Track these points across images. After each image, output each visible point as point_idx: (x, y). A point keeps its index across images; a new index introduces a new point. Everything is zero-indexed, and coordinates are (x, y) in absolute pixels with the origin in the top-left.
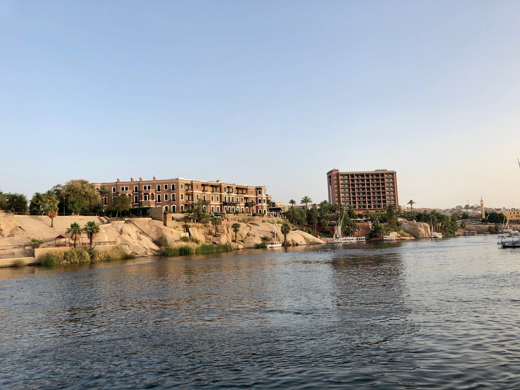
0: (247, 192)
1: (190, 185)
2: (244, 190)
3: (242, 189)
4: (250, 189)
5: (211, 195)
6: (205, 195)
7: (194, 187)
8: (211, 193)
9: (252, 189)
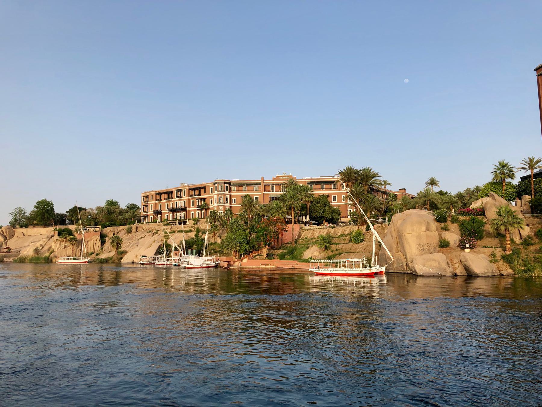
0: (205, 192)
1: (148, 196)
2: (201, 190)
3: (199, 189)
4: (209, 187)
5: (166, 204)
6: (161, 204)
7: (150, 197)
8: (165, 201)
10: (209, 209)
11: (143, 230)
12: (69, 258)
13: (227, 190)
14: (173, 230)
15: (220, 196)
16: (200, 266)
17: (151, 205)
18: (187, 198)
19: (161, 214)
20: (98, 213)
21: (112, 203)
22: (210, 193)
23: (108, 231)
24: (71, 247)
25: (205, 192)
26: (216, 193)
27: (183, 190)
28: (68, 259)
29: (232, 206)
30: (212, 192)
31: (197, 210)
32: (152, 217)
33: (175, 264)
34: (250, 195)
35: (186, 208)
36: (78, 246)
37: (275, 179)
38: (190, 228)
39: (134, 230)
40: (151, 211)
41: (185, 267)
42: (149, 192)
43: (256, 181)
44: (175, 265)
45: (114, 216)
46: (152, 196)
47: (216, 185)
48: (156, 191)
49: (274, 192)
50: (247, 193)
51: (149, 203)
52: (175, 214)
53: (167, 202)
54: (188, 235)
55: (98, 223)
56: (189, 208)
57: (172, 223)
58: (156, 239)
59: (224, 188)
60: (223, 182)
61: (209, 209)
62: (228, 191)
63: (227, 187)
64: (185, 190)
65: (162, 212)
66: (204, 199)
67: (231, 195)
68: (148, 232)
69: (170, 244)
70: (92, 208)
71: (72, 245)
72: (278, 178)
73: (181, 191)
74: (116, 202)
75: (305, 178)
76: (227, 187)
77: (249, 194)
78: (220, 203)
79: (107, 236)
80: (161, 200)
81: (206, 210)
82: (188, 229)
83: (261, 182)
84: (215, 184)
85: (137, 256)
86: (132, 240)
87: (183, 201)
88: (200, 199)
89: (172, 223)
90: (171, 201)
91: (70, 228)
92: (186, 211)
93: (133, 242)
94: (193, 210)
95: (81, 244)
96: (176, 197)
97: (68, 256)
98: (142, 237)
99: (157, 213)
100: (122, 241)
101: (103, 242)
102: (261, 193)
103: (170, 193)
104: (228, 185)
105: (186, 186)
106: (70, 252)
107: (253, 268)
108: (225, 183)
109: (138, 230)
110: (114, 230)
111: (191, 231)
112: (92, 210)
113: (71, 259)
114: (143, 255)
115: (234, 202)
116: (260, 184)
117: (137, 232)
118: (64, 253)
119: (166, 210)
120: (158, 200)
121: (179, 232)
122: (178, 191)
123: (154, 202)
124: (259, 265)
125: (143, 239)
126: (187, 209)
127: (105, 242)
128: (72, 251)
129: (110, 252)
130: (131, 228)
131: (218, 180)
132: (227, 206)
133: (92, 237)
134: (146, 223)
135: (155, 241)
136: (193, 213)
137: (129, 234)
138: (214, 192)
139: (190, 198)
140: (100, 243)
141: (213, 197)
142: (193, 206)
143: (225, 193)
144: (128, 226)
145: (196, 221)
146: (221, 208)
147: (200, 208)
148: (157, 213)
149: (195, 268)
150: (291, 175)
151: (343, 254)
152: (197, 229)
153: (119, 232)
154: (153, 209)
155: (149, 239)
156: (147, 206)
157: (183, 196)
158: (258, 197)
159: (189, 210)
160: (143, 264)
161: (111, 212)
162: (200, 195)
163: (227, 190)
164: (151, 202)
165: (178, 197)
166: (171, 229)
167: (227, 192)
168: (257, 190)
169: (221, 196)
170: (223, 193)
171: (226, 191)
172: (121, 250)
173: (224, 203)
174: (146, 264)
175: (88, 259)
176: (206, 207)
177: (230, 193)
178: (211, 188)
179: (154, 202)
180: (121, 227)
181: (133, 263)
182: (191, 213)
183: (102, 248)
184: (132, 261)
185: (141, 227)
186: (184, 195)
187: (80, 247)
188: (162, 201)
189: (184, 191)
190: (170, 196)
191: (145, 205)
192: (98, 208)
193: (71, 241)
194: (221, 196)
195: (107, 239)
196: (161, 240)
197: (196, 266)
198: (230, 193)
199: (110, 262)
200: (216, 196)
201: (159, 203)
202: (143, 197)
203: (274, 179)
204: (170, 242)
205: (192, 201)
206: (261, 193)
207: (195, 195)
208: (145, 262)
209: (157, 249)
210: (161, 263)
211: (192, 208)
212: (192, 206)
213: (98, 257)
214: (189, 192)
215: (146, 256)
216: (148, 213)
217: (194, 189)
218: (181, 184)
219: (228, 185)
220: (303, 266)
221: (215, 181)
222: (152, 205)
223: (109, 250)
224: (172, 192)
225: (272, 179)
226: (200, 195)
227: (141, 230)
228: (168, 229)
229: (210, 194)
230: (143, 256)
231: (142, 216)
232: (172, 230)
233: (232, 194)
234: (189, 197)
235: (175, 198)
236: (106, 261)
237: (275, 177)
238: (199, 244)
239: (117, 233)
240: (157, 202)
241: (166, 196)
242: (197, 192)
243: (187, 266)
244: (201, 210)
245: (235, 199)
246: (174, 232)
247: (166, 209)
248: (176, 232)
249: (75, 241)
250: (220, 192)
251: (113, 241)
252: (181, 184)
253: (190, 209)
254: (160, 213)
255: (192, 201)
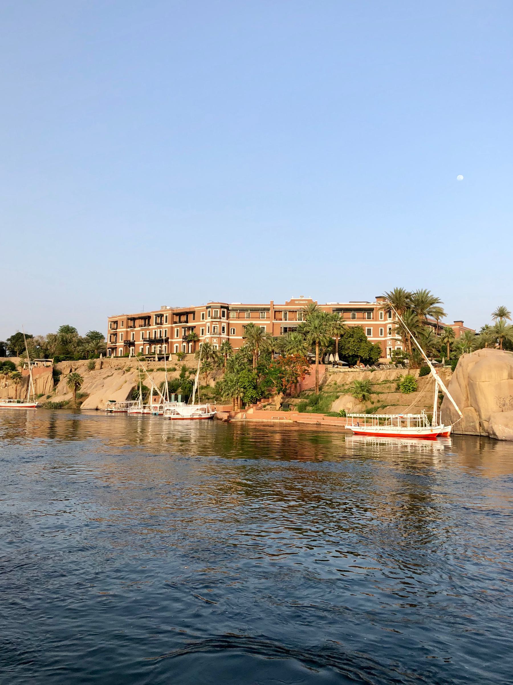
0: (194, 319)
1: (117, 321)
2: (189, 315)
3: (187, 314)
5: (141, 332)
6: (134, 332)
7: (120, 323)
8: (139, 329)
9: (202, 311)
10: (199, 341)
11: (109, 367)
12: (12, 400)
13: (224, 316)
14: (151, 367)
15: (214, 324)
16: (189, 417)
17: (120, 333)
18: (170, 325)
19: (134, 346)
20: (49, 343)
21: (67, 330)
22: (201, 320)
23: (63, 366)
24: (14, 386)
25: (194, 319)
26: (209, 319)
27: (165, 315)
28: (10, 402)
29: (230, 337)
30: (203, 319)
31: (183, 342)
32: (122, 349)
33: (155, 413)
34: (255, 324)
35: (168, 338)
36: (23, 385)
37: (289, 303)
38: (174, 366)
39: (97, 366)
40: (120, 341)
41: (170, 417)
42: (119, 316)
43: (262, 305)
44: (155, 414)
45: (71, 347)
46: (123, 321)
47: (210, 309)
48: (128, 316)
49: (287, 321)
50: (251, 322)
51: (118, 330)
52: (153, 346)
53: (142, 330)
54: (170, 375)
55: (49, 356)
56: (172, 339)
57: (150, 358)
58: (128, 379)
59: (220, 314)
60: (219, 306)
61: (199, 341)
62: (225, 318)
63: (224, 312)
64: (168, 315)
65: (136, 343)
66: (192, 328)
67: (229, 324)
68: (116, 369)
69: (147, 386)
70: (42, 335)
71: (16, 383)
72: (292, 302)
73: (161, 316)
74: (73, 329)
75: (330, 304)
76: (224, 312)
77: (254, 322)
78: (214, 333)
79: (61, 373)
80: (135, 328)
81: (195, 342)
82: (171, 367)
83: (269, 306)
84: (208, 308)
85: (102, 400)
86: (96, 380)
87: (164, 330)
88: (186, 327)
89: (150, 358)
90: (149, 329)
91: (13, 361)
92: (168, 343)
93: (97, 382)
94: (177, 341)
95: (27, 382)
96: (154, 324)
97: (9, 398)
98: (108, 376)
99: (130, 344)
100: (83, 381)
101: (56, 381)
102: (269, 322)
103: (147, 318)
104: (225, 310)
105: (168, 310)
106: (12, 393)
107: (262, 422)
108: (222, 307)
109: (103, 367)
110: (71, 365)
111: (175, 370)
112: (42, 338)
113: (14, 402)
114: (111, 400)
115: (232, 333)
116: (268, 309)
117: (101, 368)
118: (5, 394)
119: (141, 341)
120: (131, 327)
121: (158, 370)
122: (157, 316)
123: (125, 330)
124: (271, 419)
125: (109, 378)
126: (169, 340)
127: (59, 381)
128: (15, 392)
129: (65, 394)
130: (94, 363)
131: (212, 303)
132: (224, 338)
133: (42, 374)
134: (114, 357)
135: (126, 382)
136: (177, 346)
137: (92, 372)
138: (206, 319)
139: (174, 325)
140: (53, 381)
141: (205, 325)
142: (177, 336)
143: (221, 320)
144: (90, 360)
145: (182, 356)
146: (215, 340)
147: (187, 339)
148: (130, 344)
149: (183, 419)
150: (310, 298)
151: (388, 407)
152: (183, 367)
153: (77, 368)
154: (124, 339)
155: (118, 378)
156: (115, 334)
157: (165, 323)
158: (265, 326)
159: (172, 342)
160: (111, 412)
161: (66, 342)
162: (187, 322)
163: (224, 316)
164: (122, 330)
165: (158, 324)
166: (148, 366)
167: (224, 319)
168: (264, 318)
169: (216, 324)
170: (219, 320)
171: (222, 318)
172: (80, 392)
173: (220, 334)
174: (115, 412)
175: (37, 403)
176: (196, 339)
177: (227, 321)
178: (201, 313)
179: (125, 330)
180: (81, 362)
181: (97, 409)
182: (175, 345)
183: (55, 389)
184: (95, 407)
185: (107, 362)
186: (166, 322)
187: (26, 386)
188: (135, 329)
189: (166, 316)
190: (147, 323)
191: (113, 333)
192: (50, 336)
193: (14, 379)
194: (216, 324)
195: (61, 377)
196: (134, 380)
197: (184, 417)
198: (227, 321)
199: (66, 407)
200: (208, 324)
201: (132, 331)
202: (110, 323)
203: (287, 304)
204: (147, 383)
205: (176, 329)
206: (269, 322)
207: (180, 322)
208: (114, 410)
209: (130, 392)
210: (135, 411)
211: (176, 339)
212: (176, 337)
213: (49, 400)
214: (173, 318)
215: (115, 401)
216: (117, 344)
217: (180, 315)
218: (162, 307)
219: (226, 309)
220: (332, 421)
221: (208, 304)
222: (123, 333)
223: (65, 392)
224: (149, 318)
225: (285, 304)
226: (187, 323)
227: (107, 366)
228: (144, 365)
229: (200, 322)
230: (111, 401)
231: (108, 348)
232: (149, 367)
233: (231, 322)
234: (172, 324)
235: (153, 326)
236: (60, 406)
237: (289, 301)
238: (186, 388)
239: (75, 369)
240: (129, 329)
241: (142, 322)
242: (184, 318)
243: (172, 416)
244: (188, 342)
245: (234, 329)
246: (152, 370)
247: (141, 339)
248: (155, 370)
249: (20, 378)
250: (215, 318)
251: (70, 380)
252: (162, 307)
253: (173, 340)
254: (132, 344)
255: (176, 329)
